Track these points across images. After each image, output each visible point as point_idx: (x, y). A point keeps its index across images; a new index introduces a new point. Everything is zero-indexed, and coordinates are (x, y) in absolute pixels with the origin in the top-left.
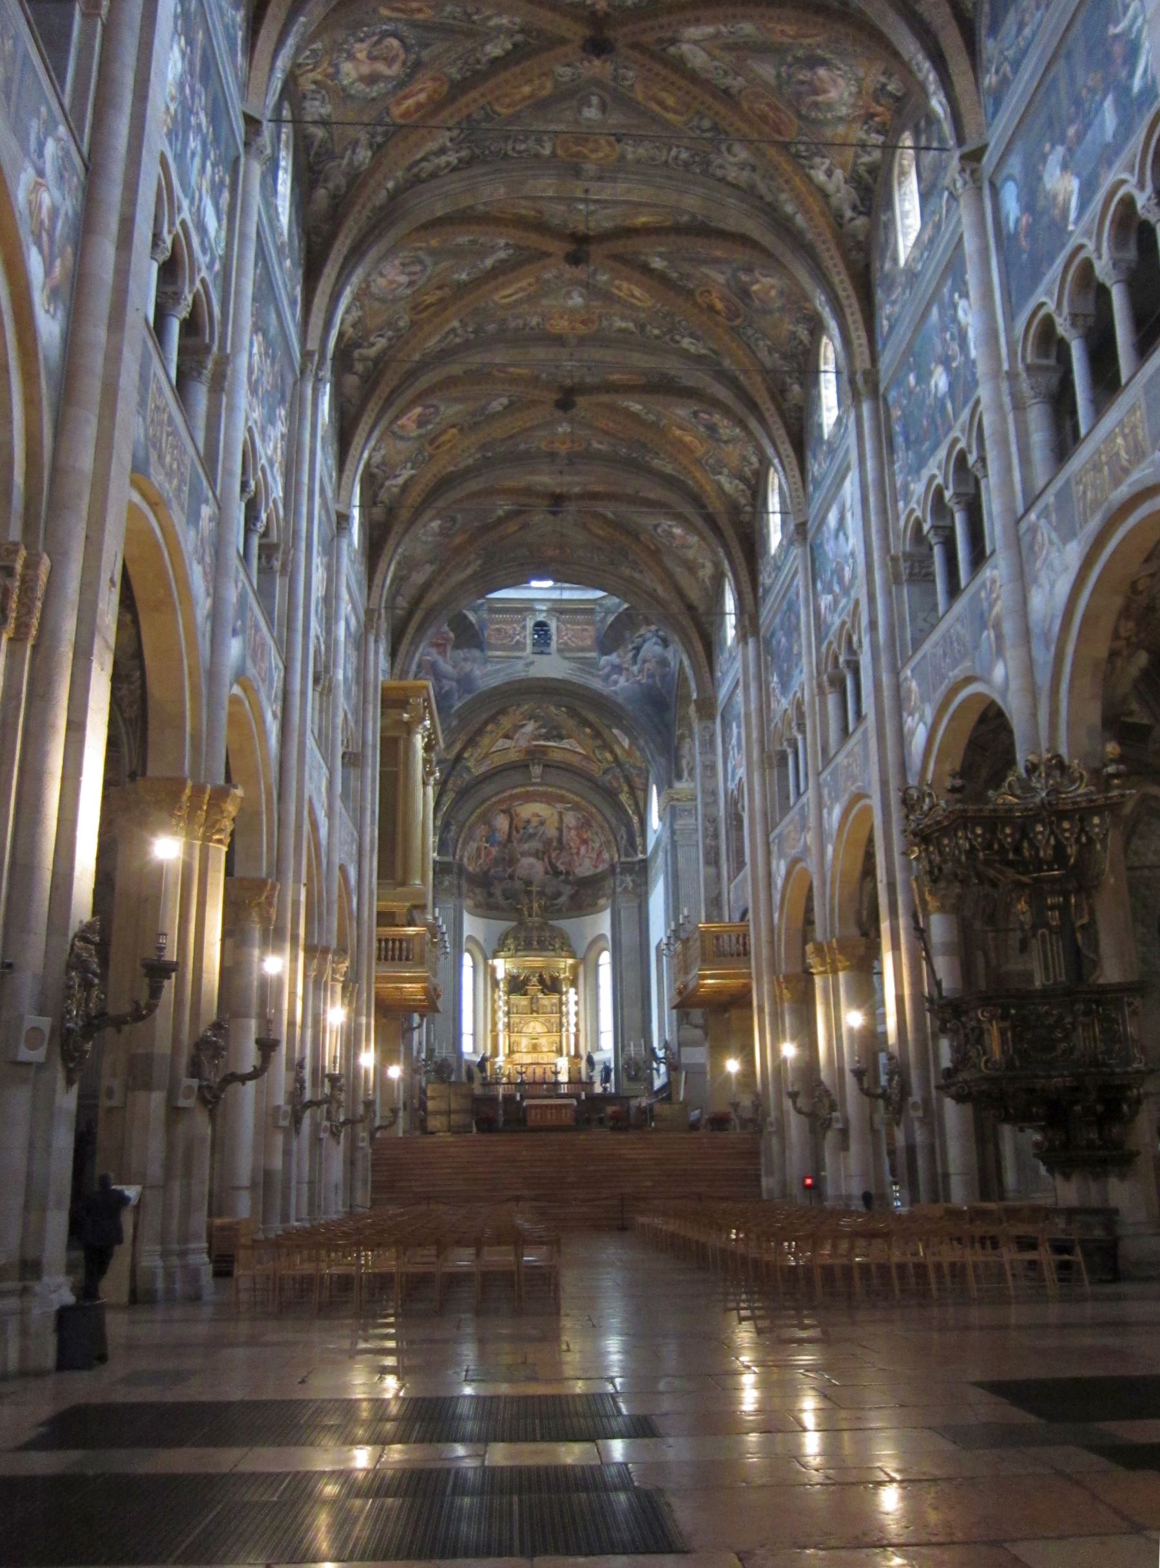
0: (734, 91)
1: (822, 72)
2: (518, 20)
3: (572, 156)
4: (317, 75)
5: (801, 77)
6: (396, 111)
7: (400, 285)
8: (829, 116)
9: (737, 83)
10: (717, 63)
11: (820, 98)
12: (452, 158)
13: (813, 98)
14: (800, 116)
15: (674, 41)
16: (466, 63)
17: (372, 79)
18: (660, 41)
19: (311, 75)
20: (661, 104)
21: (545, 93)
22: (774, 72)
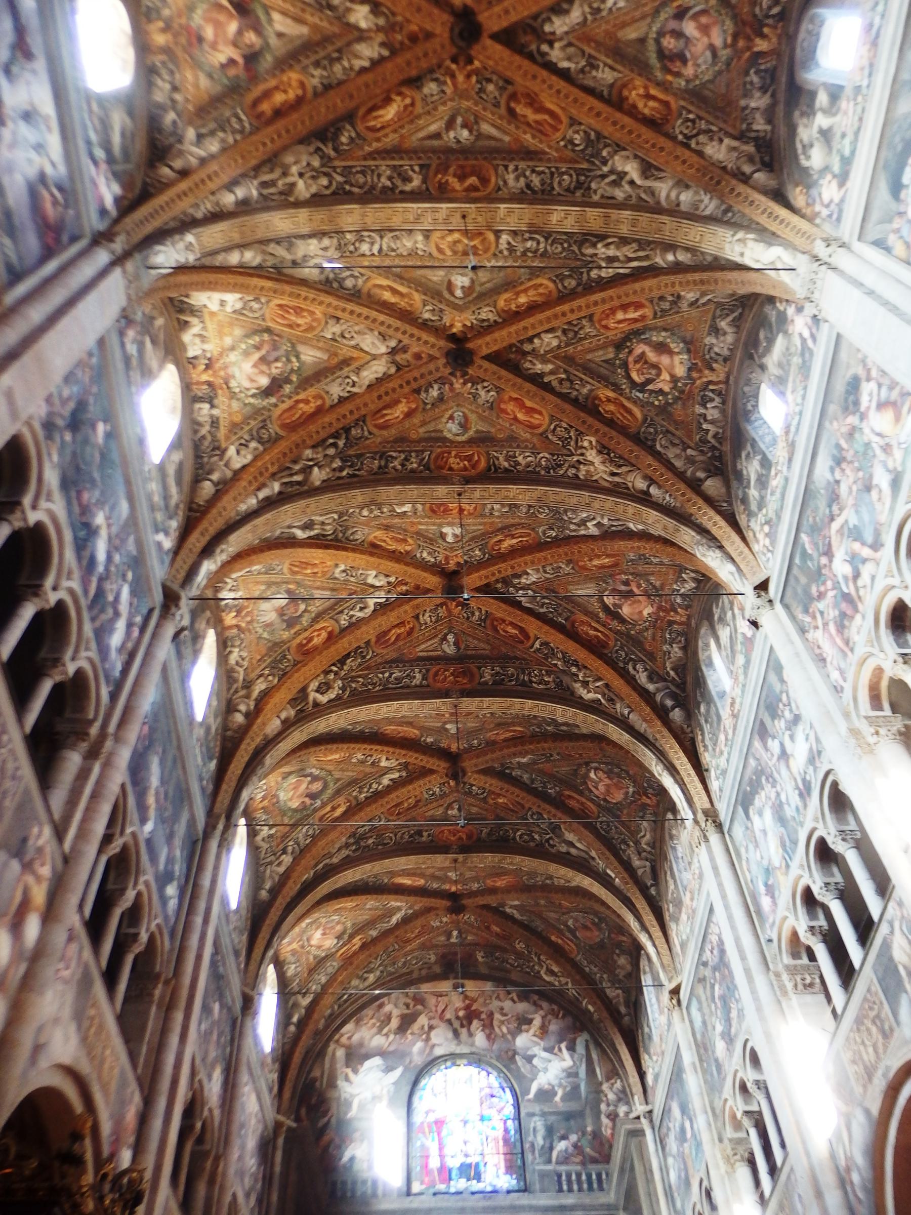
0: (332, 322)
1: (264, 381)
2: (527, 365)
3: (481, 234)
4: (709, 376)
5: (279, 365)
6: (648, 312)
7: (695, 17)
8: (243, 346)
9: (334, 329)
10: (353, 343)
11: (257, 356)
12: (601, 250)
13: (263, 352)
14: (268, 330)
15: (393, 352)
16: (576, 333)
17: (661, 348)
18: (405, 350)
19: (713, 378)
20: (394, 291)
21: (506, 296)
22: (303, 357)
